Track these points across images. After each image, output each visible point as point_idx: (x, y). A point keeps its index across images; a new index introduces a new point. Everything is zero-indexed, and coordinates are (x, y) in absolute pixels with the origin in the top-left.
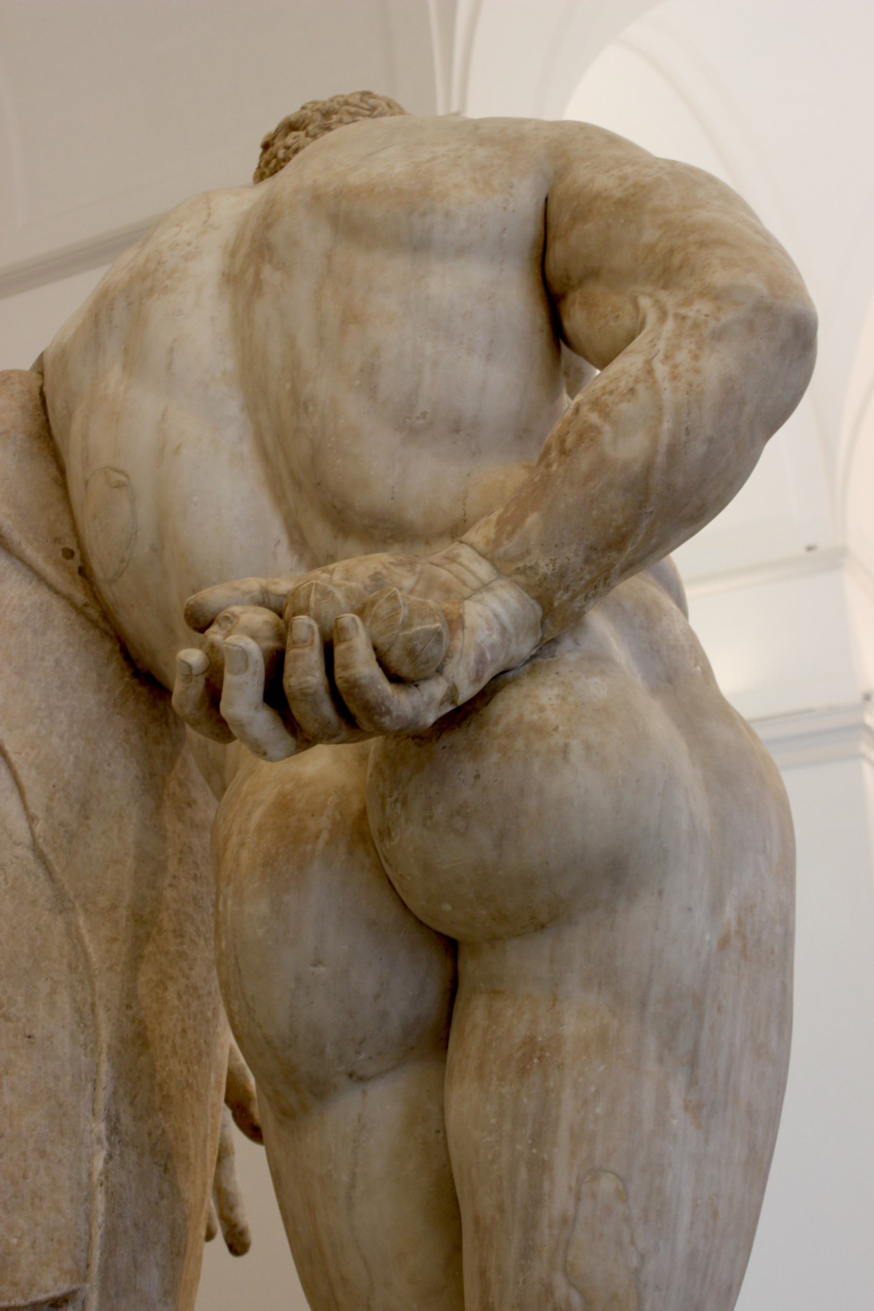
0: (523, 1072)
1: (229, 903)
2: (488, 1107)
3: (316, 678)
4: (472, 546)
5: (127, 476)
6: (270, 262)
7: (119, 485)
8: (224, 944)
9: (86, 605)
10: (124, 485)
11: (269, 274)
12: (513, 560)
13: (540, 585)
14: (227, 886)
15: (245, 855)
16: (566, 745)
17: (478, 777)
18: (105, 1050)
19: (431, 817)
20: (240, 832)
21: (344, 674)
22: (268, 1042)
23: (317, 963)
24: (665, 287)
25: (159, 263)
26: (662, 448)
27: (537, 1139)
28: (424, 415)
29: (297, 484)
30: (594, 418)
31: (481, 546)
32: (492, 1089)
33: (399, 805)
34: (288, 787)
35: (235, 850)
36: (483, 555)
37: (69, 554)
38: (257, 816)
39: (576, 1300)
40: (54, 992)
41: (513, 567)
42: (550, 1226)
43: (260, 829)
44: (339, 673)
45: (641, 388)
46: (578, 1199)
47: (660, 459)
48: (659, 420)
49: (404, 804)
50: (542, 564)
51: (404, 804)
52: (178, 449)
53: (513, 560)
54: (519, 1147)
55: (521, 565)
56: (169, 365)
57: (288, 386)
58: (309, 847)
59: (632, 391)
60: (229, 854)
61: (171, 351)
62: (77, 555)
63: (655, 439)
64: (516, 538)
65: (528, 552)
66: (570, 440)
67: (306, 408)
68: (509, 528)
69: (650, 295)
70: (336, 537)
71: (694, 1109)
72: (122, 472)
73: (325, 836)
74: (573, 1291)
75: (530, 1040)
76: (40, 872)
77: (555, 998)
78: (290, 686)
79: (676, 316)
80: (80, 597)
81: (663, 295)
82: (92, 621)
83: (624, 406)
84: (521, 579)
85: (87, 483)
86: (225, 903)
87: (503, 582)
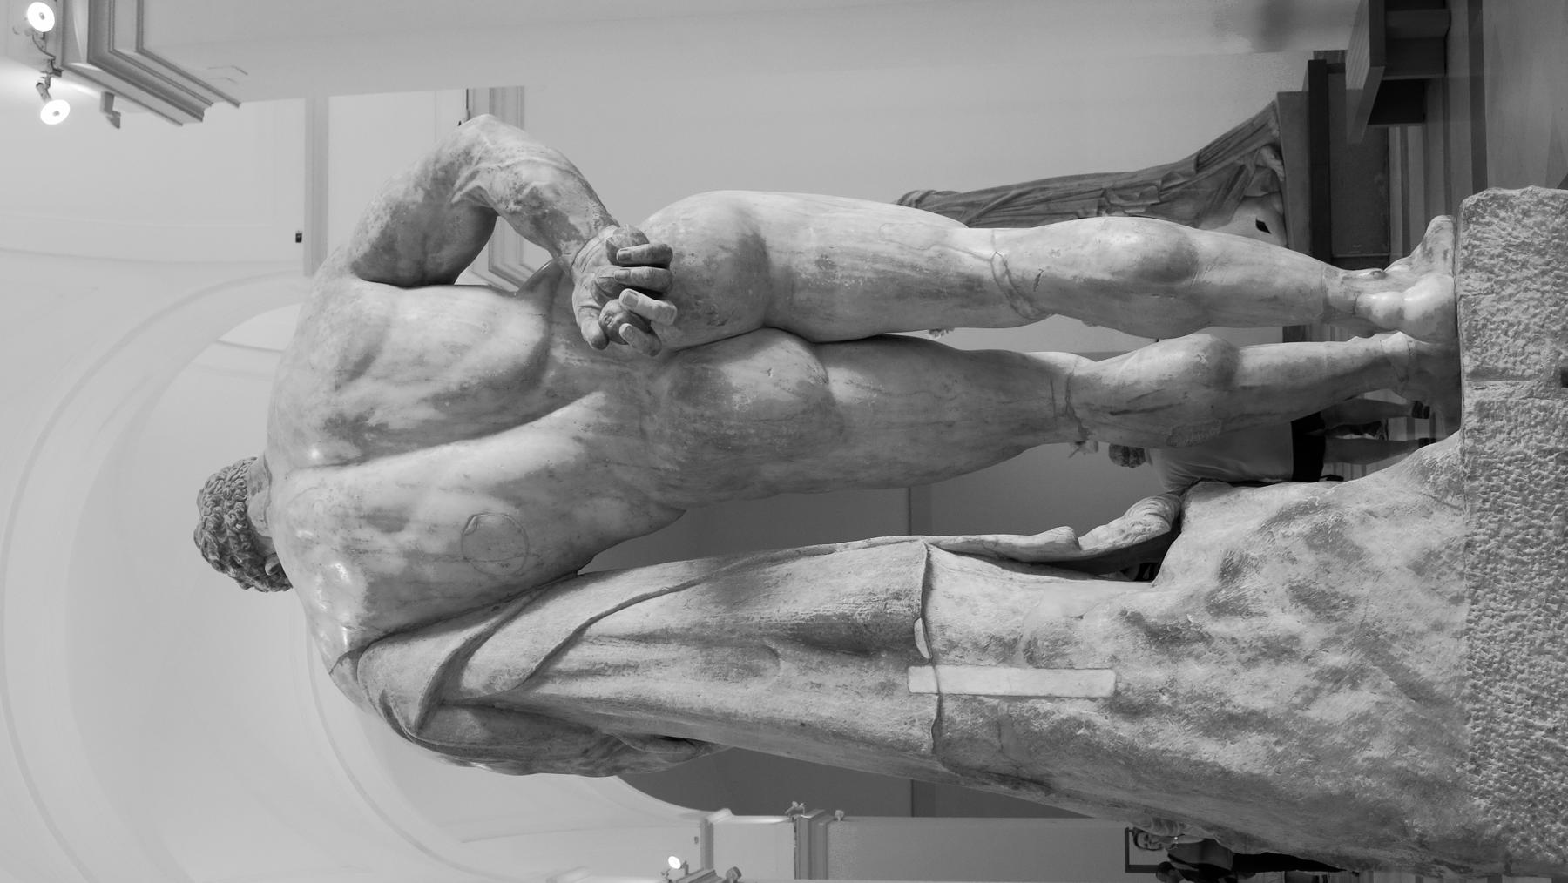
0: (833, 266)
1: (732, 423)
2: (847, 285)
3: (646, 269)
4: (578, 253)
5: (473, 516)
6: (367, 420)
7: (477, 523)
8: (752, 431)
9: (531, 596)
10: (476, 519)
11: (372, 422)
12: (590, 230)
13: (604, 221)
14: (722, 426)
15: (708, 413)
16: (683, 220)
17: (693, 255)
18: (796, 549)
19: (708, 281)
20: (695, 422)
21: (646, 254)
22: (804, 412)
23: (769, 371)
24: (453, 184)
25: (340, 506)
26: (549, 162)
27: (863, 258)
28: (484, 325)
29: (502, 409)
30: (526, 191)
31: (579, 247)
32: (838, 282)
33: (699, 302)
34: (675, 394)
35: (704, 422)
36: (585, 244)
37: (496, 608)
38: (689, 410)
39: (936, 248)
40: (764, 573)
41: (594, 230)
42: (903, 254)
43: (696, 405)
44: (642, 261)
45: (515, 170)
46: (891, 241)
47: (554, 163)
48: (534, 162)
49: (698, 297)
50: (594, 217)
51: (698, 297)
52: (466, 477)
53: (590, 230)
54: (866, 268)
55: (593, 227)
56: (412, 486)
57: (447, 404)
58: (710, 372)
59: (516, 174)
60: (705, 429)
61: (403, 486)
62: (498, 605)
63: (543, 164)
64: (579, 228)
65: (588, 223)
66: (535, 203)
67: (465, 388)
68: (573, 233)
69: (455, 194)
70: (538, 387)
71: (855, 208)
72: (470, 520)
73: (704, 365)
74: (932, 248)
75: (818, 263)
76: (692, 588)
77: (800, 253)
78: (648, 279)
79: (477, 164)
80: (525, 599)
81: (457, 185)
82: (541, 595)
83: (523, 177)
84: (600, 228)
85: (466, 559)
86: (731, 427)
87: (600, 234)
